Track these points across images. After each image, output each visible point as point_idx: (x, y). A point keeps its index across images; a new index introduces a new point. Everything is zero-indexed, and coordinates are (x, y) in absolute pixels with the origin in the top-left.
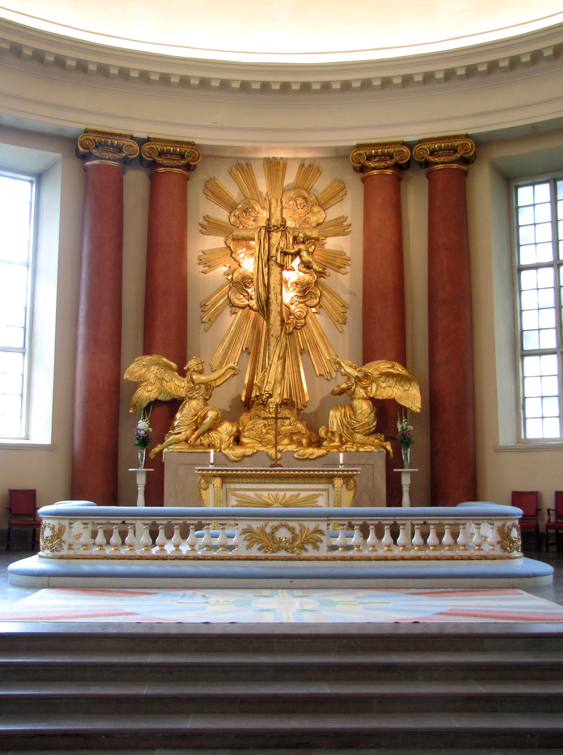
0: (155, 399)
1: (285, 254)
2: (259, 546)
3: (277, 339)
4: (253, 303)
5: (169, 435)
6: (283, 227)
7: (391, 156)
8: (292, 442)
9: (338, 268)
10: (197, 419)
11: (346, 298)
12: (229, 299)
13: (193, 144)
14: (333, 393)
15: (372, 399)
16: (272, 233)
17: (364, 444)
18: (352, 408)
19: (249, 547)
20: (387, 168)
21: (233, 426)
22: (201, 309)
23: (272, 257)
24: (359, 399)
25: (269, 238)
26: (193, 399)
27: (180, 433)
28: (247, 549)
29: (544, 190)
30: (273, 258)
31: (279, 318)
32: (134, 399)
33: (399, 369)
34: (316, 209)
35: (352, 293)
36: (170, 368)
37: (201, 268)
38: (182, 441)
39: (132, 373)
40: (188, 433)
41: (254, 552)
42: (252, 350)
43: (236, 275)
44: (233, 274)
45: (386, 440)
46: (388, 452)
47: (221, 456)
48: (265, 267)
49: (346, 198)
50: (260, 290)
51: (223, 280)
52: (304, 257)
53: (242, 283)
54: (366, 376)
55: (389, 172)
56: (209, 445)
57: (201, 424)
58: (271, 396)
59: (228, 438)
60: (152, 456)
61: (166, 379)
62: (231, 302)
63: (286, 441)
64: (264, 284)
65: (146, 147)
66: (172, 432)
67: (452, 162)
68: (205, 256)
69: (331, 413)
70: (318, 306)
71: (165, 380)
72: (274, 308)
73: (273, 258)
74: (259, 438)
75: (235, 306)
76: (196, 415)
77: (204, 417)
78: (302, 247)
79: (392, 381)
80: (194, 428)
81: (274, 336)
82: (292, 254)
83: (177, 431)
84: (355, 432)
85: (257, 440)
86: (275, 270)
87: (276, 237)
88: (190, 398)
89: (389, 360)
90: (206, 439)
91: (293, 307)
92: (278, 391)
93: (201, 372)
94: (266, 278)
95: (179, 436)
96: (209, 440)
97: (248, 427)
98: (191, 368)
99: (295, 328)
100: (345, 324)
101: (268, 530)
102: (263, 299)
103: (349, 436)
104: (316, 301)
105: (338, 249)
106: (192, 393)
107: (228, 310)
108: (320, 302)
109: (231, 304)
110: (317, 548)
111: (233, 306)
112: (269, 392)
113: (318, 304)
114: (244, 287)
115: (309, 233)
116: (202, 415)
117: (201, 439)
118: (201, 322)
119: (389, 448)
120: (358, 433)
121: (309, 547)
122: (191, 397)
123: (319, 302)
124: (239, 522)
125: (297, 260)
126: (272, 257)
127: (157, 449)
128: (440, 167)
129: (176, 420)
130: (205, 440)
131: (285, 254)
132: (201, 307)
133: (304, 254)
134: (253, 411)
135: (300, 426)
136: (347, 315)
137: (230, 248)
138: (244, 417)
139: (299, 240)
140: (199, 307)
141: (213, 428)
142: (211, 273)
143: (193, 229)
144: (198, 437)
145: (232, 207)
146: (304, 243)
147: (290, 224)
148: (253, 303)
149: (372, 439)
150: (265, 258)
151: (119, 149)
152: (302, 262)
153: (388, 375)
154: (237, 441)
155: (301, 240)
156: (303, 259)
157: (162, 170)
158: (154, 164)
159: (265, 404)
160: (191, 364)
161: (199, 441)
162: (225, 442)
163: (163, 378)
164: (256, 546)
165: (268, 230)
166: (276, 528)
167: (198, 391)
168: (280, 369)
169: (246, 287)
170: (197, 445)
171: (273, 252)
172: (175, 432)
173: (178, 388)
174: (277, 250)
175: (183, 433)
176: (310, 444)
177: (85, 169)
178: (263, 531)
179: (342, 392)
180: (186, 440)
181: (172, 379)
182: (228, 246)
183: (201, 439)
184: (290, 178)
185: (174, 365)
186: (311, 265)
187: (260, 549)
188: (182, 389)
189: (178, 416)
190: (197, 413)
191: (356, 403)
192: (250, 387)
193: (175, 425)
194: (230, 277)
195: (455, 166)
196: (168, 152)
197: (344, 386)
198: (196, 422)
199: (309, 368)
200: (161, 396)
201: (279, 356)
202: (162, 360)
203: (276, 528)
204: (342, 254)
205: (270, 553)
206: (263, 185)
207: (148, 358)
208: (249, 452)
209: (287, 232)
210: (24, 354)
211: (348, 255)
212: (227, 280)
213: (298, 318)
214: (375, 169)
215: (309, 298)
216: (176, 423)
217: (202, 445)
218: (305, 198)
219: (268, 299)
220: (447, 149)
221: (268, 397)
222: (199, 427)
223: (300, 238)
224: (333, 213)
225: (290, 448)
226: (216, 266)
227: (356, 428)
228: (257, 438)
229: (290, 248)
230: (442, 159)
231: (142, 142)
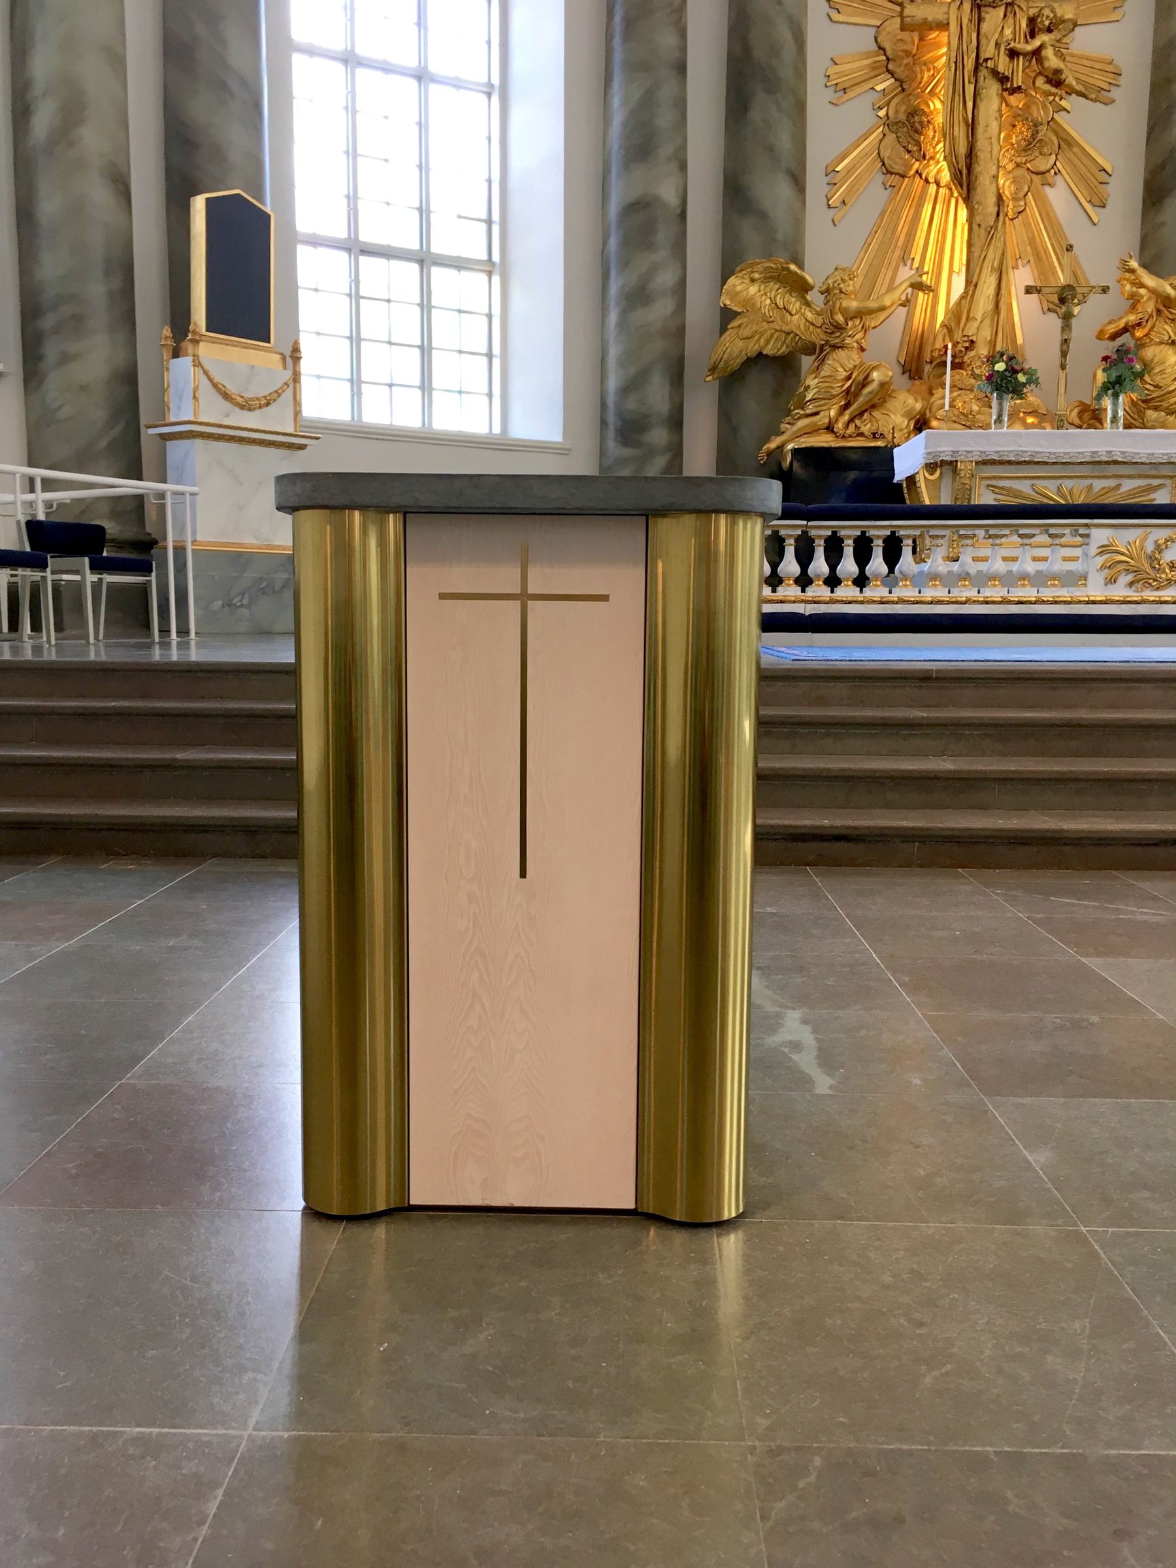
0: (757, 353)
1: (1013, 54)
2: (1130, 578)
3: (989, 233)
5: (793, 418)
10: (851, 386)
16: (987, 9)
21: (916, 400)
22: (827, 180)
23: (986, 60)
24: (1161, 343)
25: (980, 20)
26: (840, 347)
27: (816, 414)
28: (1106, 585)
30: (990, 64)
31: (994, 188)
38: (819, 429)
39: (734, 295)
40: (833, 413)
44: (888, 104)
48: (970, 82)
50: (956, 133)
52: (1047, 58)
53: (908, 124)
56: (874, 434)
57: (857, 395)
59: (906, 422)
61: (790, 308)
62: (884, 164)
64: (966, 120)
66: (802, 412)
68: (837, 69)
70: (1052, 172)
71: (787, 311)
73: (989, 62)
74: (968, 421)
75: (891, 173)
76: (849, 378)
77: (865, 383)
80: (842, 403)
81: (983, 226)
82: (1025, 55)
83: (810, 409)
84: (1149, 408)
85: (964, 425)
88: (835, 347)
90: (866, 425)
94: (970, 105)
95: (818, 417)
96: (872, 426)
98: (834, 287)
101: (1150, 547)
102: (962, 149)
103: (1136, 416)
106: (838, 337)
107: (880, 178)
108: (1057, 163)
109: (883, 167)
112: (971, 338)
113: (1053, 168)
114: (912, 133)
116: (861, 378)
117: (856, 425)
118: (825, 206)
120: (1156, 409)
122: (837, 343)
123: (1055, 164)
124: (1094, 532)
126: (986, 60)
129: (807, 388)
130: (865, 426)
132: (827, 175)
133: (1049, 53)
137: (884, 50)
139: (1042, 21)
140: (824, 174)
144: (851, 420)
146: (1049, 30)
150: (970, 63)
155: (1047, 23)
156: (1046, 64)
161: (852, 428)
162: (901, 430)
163: (784, 307)
164: (1124, 579)
167: (850, 333)
169: (916, 131)
170: (850, 436)
172: (808, 411)
173: (811, 327)
174: (997, 45)
175: (822, 414)
180: (830, 428)
181: (801, 308)
182: (880, 48)
183: (856, 425)
186: (1063, 77)
187: (1131, 584)
188: (818, 330)
189: (812, 382)
190: (851, 374)
193: (807, 399)
194: (882, 113)
198: (848, 391)
200: (770, 347)
201: (992, 267)
202: (788, 269)
205: (1152, 591)
209: (1016, 8)
212: (878, 119)
215: (1037, 153)
216: (809, 397)
217: (861, 434)
221: (967, 348)
222: (852, 402)
223: (1045, 18)
227: (1153, 399)
228: (964, 421)
229: (1022, 41)
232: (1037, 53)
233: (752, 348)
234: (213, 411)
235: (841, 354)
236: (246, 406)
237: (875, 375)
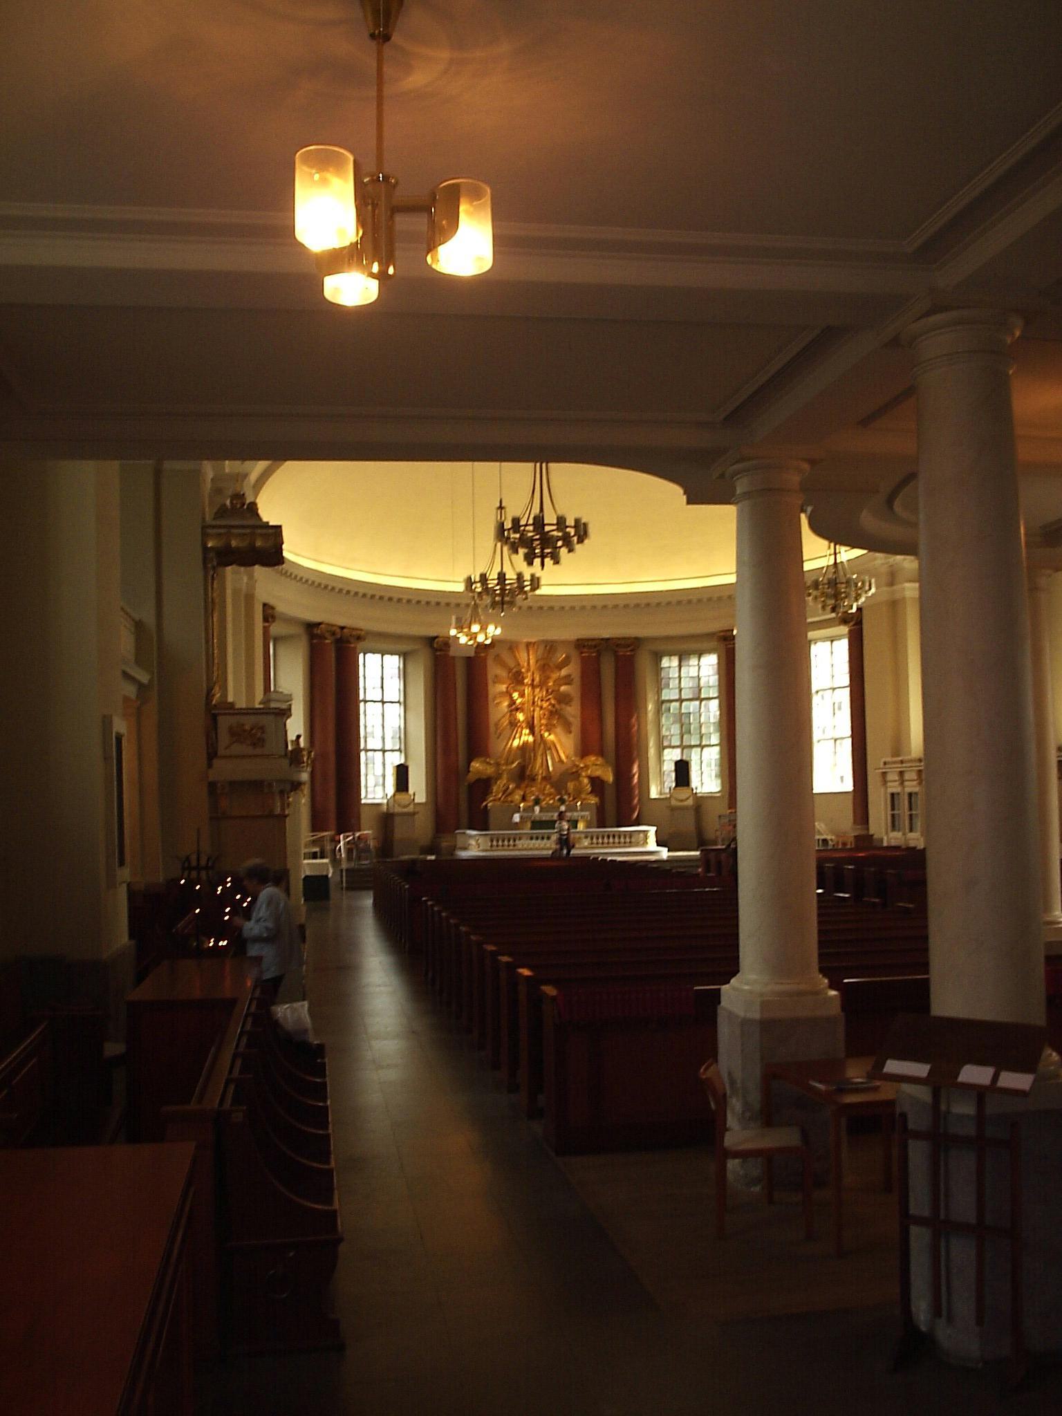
20: (593, 653)
29: (675, 662)
33: (600, 761)
69: (569, 784)
92: (540, 772)
127: (484, 804)
128: (622, 653)
134: (526, 782)
135: (552, 790)
144: (505, 798)
171: (536, 699)
180: (500, 799)
199: (553, 758)
210: (401, 752)
224: (564, 672)
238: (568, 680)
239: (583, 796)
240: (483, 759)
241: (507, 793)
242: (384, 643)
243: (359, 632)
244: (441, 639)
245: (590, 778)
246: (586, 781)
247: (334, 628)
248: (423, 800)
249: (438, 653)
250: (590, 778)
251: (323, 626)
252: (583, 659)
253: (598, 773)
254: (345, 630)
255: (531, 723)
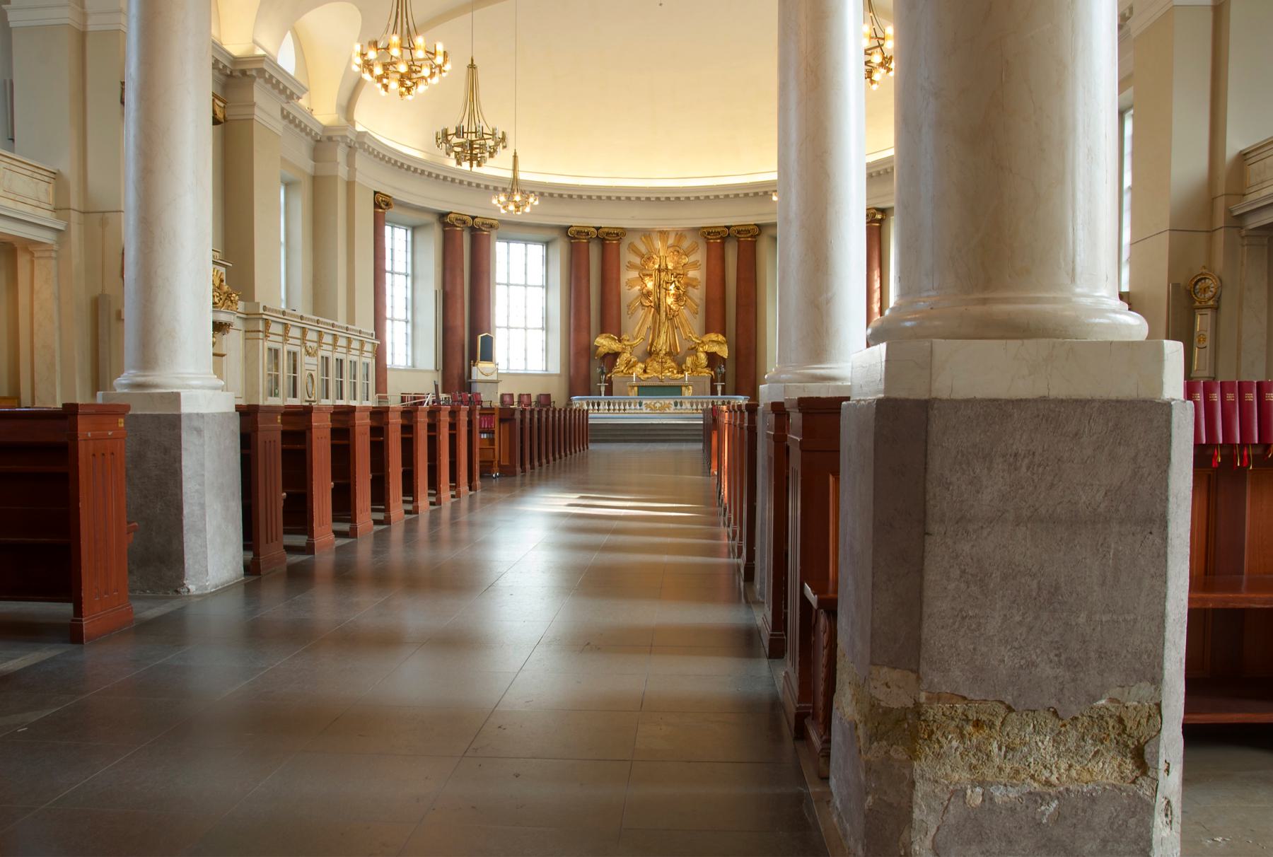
1: (667, 283)
4: (652, 304)
6: (667, 268)
7: (719, 233)
8: (669, 372)
9: (694, 287)
11: (698, 301)
12: (641, 302)
13: (622, 228)
14: (689, 349)
15: (707, 353)
17: (701, 372)
18: (697, 356)
19: (646, 409)
32: (597, 353)
33: (721, 338)
34: (683, 257)
35: (701, 299)
36: (615, 340)
37: (627, 287)
39: (598, 342)
41: (648, 411)
42: (652, 327)
43: (644, 291)
45: (712, 370)
46: (712, 376)
47: (638, 378)
49: (699, 251)
51: (638, 293)
54: (703, 342)
55: (719, 241)
58: (660, 350)
60: (607, 378)
63: (667, 371)
65: (600, 231)
67: (748, 237)
69: (688, 358)
72: (663, 309)
77: (631, 360)
78: (675, 279)
79: (715, 344)
86: (663, 291)
87: (663, 274)
88: (624, 352)
89: (717, 333)
91: (672, 306)
93: (628, 340)
97: (650, 365)
99: (673, 316)
100: (697, 314)
104: (683, 303)
105: (694, 277)
107: (640, 307)
110: (669, 409)
111: (643, 306)
115: (678, 272)
119: (713, 374)
121: (667, 409)
125: (673, 285)
127: (609, 375)
128: (742, 239)
131: (667, 283)
135: (673, 364)
136: (699, 310)
138: (648, 360)
141: (634, 366)
142: (632, 290)
143: (623, 268)
145: (642, 256)
147: (670, 267)
148: (652, 304)
149: (705, 370)
151: (588, 234)
152: (676, 286)
153: (713, 341)
154: (645, 371)
157: (608, 242)
158: (604, 240)
159: (658, 354)
160: (624, 336)
164: (649, 409)
165: (659, 270)
166: (655, 403)
168: (665, 338)
171: (662, 282)
176: (678, 373)
177: (571, 243)
178: (650, 403)
179: (692, 349)
180: (622, 371)
184: (671, 241)
185: (616, 338)
189: (618, 360)
191: (698, 354)
192: (652, 345)
195: (750, 239)
196: (611, 233)
197: (693, 346)
203: (655, 403)
204: (696, 279)
206: (659, 244)
207: (604, 335)
208: (649, 376)
210: (543, 330)
211: (699, 279)
213: (675, 311)
214: (711, 239)
218: (678, 252)
219: (659, 304)
220: (745, 230)
224: (692, 258)
225: (669, 374)
226: (635, 286)
230: (743, 236)
231: (598, 229)
232: (674, 281)
233: (606, 351)
234: (481, 377)
235: (625, 354)
236: (487, 375)
237: (633, 360)
238: (695, 265)
239: (699, 369)
240: (608, 335)
241: (629, 366)
242: (520, 230)
243: (492, 221)
244: (575, 228)
245: (707, 353)
246: (703, 356)
247: (465, 218)
248: (558, 372)
249: (572, 241)
250: (707, 353)
251: (452, 215)
252: (708, 243)
253: (715, 349)
254: (476, 220)
255: (657, 302)
